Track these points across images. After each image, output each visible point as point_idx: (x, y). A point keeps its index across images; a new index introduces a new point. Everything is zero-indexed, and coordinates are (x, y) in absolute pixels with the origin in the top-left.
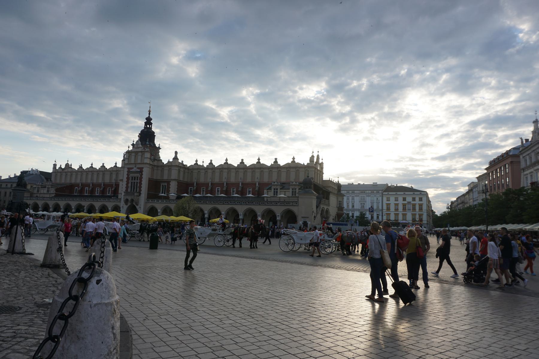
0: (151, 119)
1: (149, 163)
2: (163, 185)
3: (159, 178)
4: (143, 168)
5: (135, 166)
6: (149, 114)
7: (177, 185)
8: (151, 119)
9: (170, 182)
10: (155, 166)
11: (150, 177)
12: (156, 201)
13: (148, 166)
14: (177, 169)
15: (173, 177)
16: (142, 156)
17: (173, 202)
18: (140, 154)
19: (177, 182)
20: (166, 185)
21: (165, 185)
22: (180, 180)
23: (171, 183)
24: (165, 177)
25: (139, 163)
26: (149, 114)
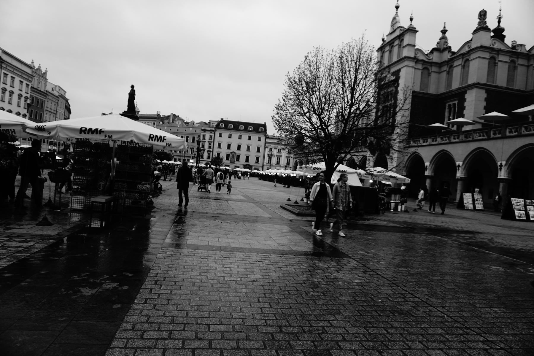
0: (503, 30)
1: (412, 55)
2: (450, 106)
3: (442, 90)
4: (399, 71)
5: (389, 72)
6: (499, 22)
7: (486, 100)
8: (503, 30)
9: (465, 93)
10: (432, 64)
11: (417, 89)
12: (421, 141)
13: (412, 64)
14: (487, 55)
15: (471, 80)
16: (400, 46)
17: (457, 140)
18: (397, 42)
19: (484, 91)
20: (456, 102)
21: (454, 104)
22: (497, 87)
23: (467, 96)
24: (456, 85)
25: (396, 62)
26: (499, 22)
